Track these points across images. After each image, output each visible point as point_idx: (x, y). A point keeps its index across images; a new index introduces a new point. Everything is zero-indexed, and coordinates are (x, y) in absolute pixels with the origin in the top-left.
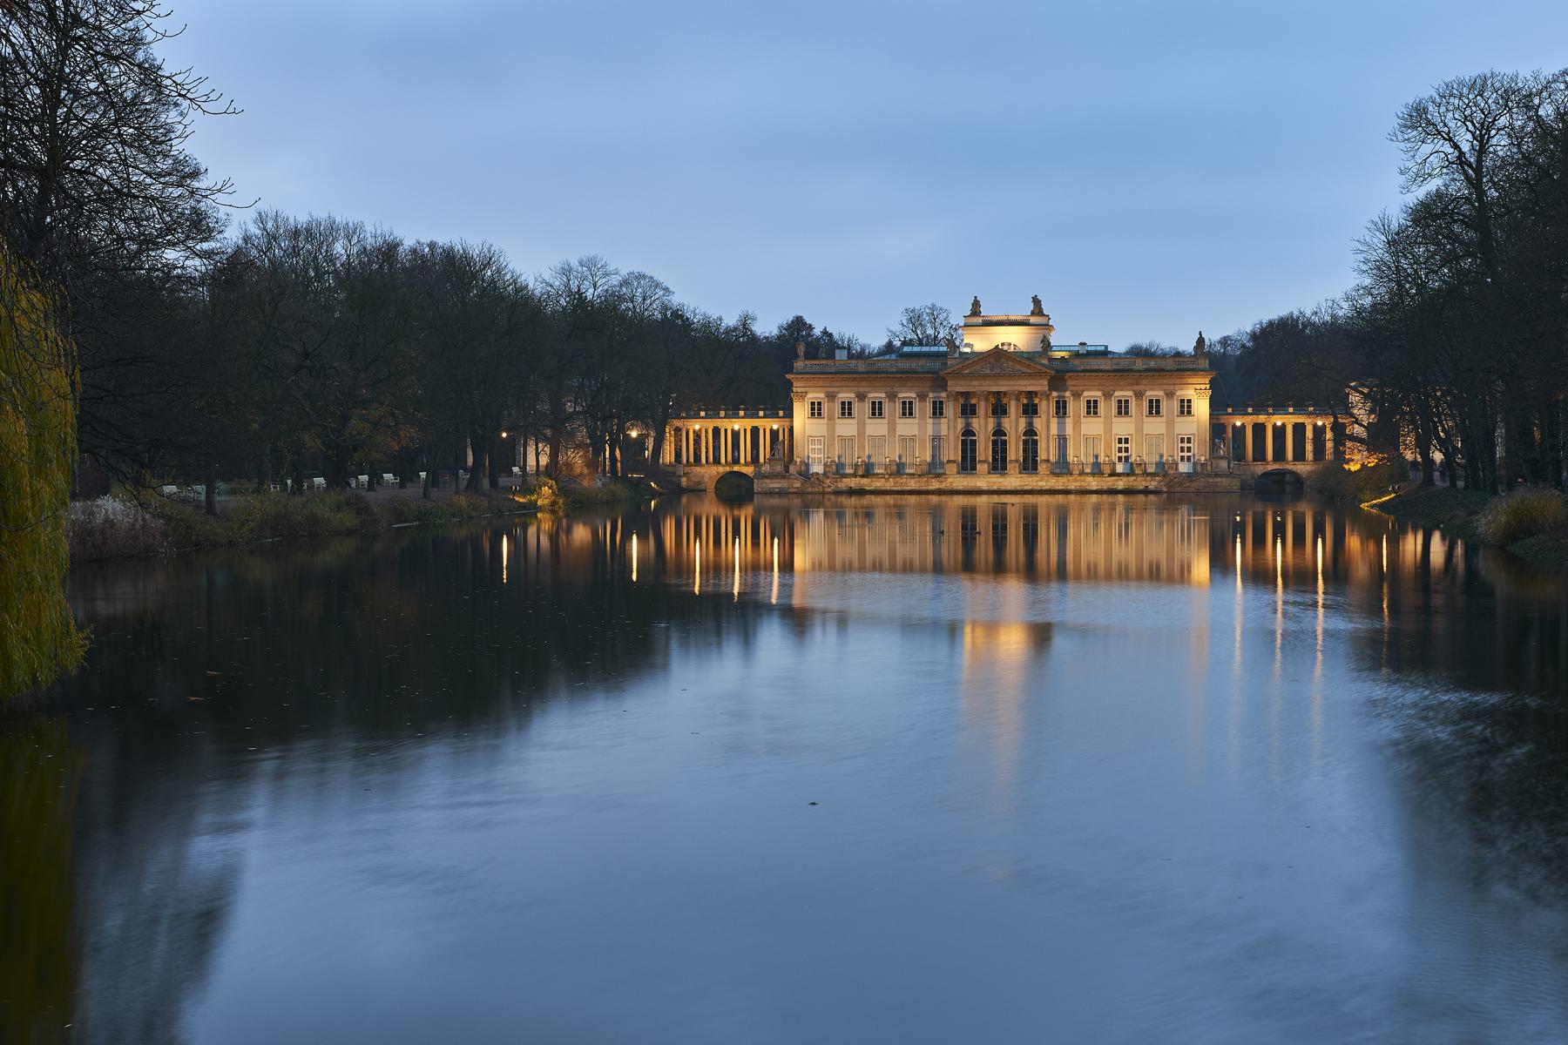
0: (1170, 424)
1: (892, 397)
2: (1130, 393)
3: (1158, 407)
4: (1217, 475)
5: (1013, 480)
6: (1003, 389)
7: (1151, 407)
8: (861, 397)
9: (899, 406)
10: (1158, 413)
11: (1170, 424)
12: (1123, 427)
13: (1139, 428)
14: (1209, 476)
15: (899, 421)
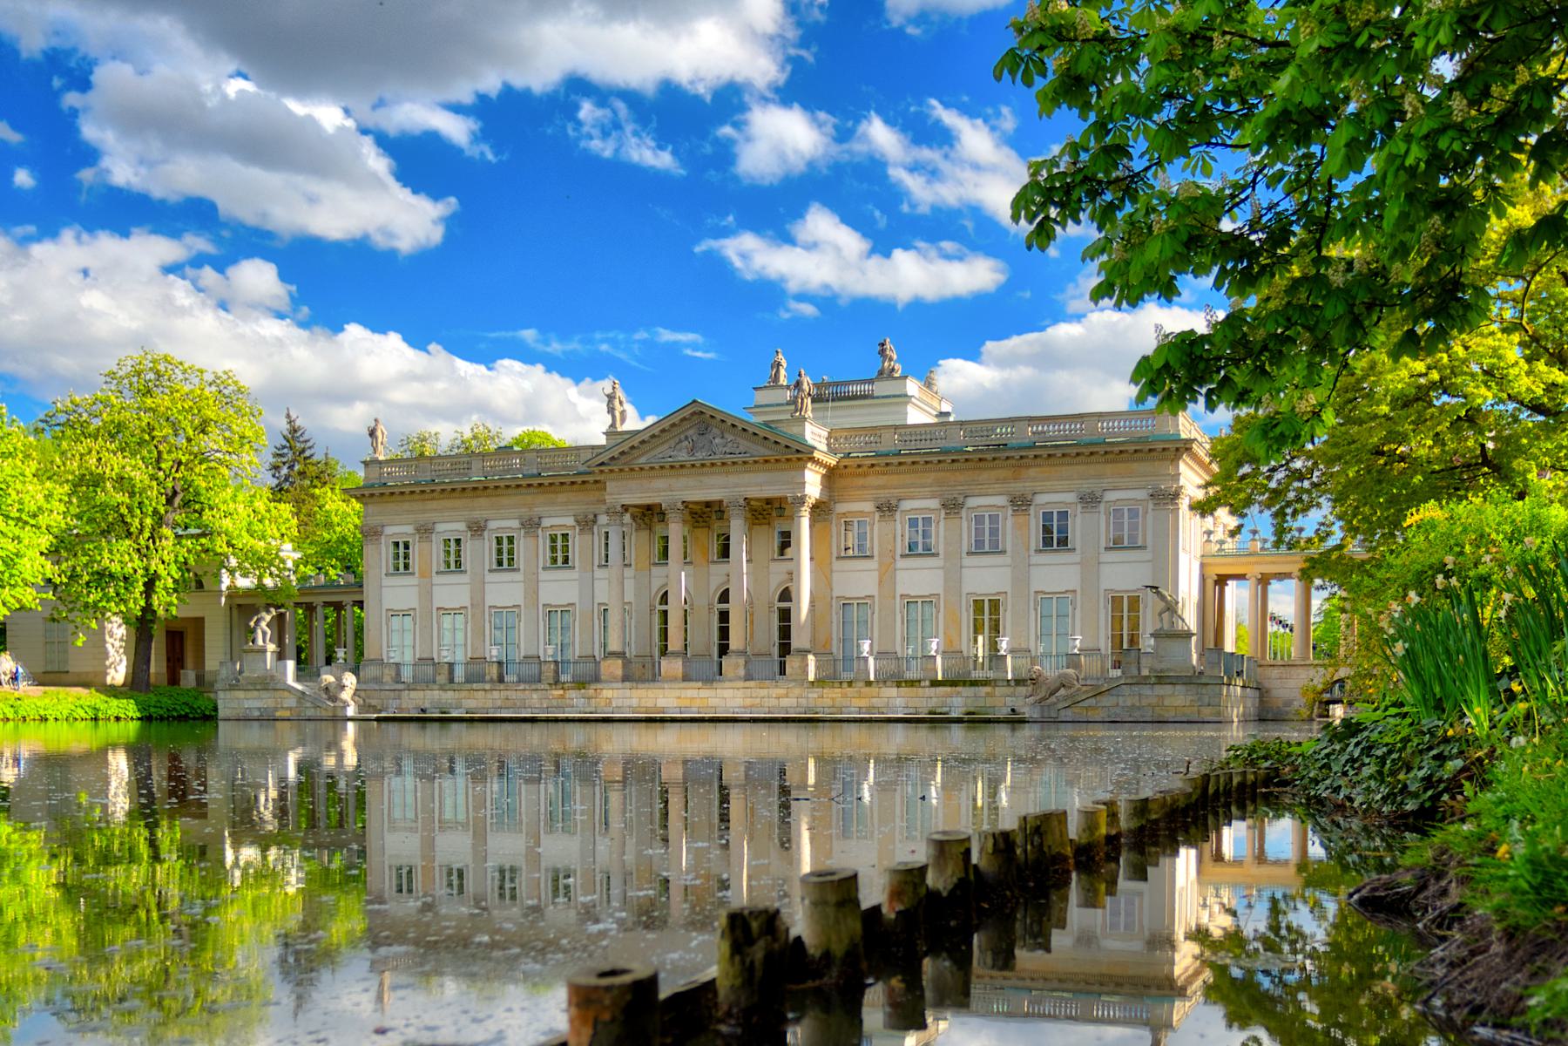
0: (1090, 570)
1: (531, 525)
2: (1001, 500)
3: (1063, 529)
4: (1161, 680)
5: (729, 697)
6: (713, 495)
7: (1047, 530)
8: (477, 529)
9: (544, 544)
10: (1063, 542)
11: (1090, 570)
12: (985, 577)
13: (1021, 579)
14: (1143, 681)
15: (543, 575)
